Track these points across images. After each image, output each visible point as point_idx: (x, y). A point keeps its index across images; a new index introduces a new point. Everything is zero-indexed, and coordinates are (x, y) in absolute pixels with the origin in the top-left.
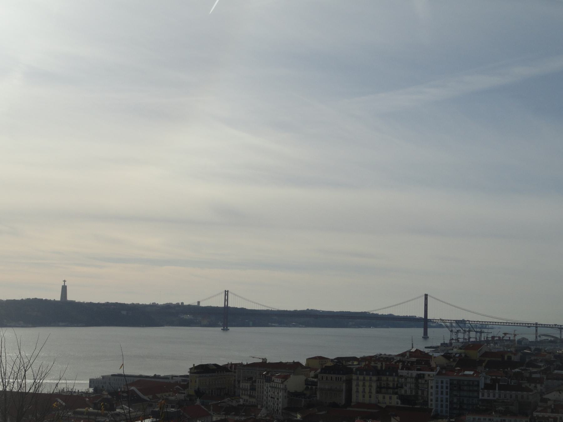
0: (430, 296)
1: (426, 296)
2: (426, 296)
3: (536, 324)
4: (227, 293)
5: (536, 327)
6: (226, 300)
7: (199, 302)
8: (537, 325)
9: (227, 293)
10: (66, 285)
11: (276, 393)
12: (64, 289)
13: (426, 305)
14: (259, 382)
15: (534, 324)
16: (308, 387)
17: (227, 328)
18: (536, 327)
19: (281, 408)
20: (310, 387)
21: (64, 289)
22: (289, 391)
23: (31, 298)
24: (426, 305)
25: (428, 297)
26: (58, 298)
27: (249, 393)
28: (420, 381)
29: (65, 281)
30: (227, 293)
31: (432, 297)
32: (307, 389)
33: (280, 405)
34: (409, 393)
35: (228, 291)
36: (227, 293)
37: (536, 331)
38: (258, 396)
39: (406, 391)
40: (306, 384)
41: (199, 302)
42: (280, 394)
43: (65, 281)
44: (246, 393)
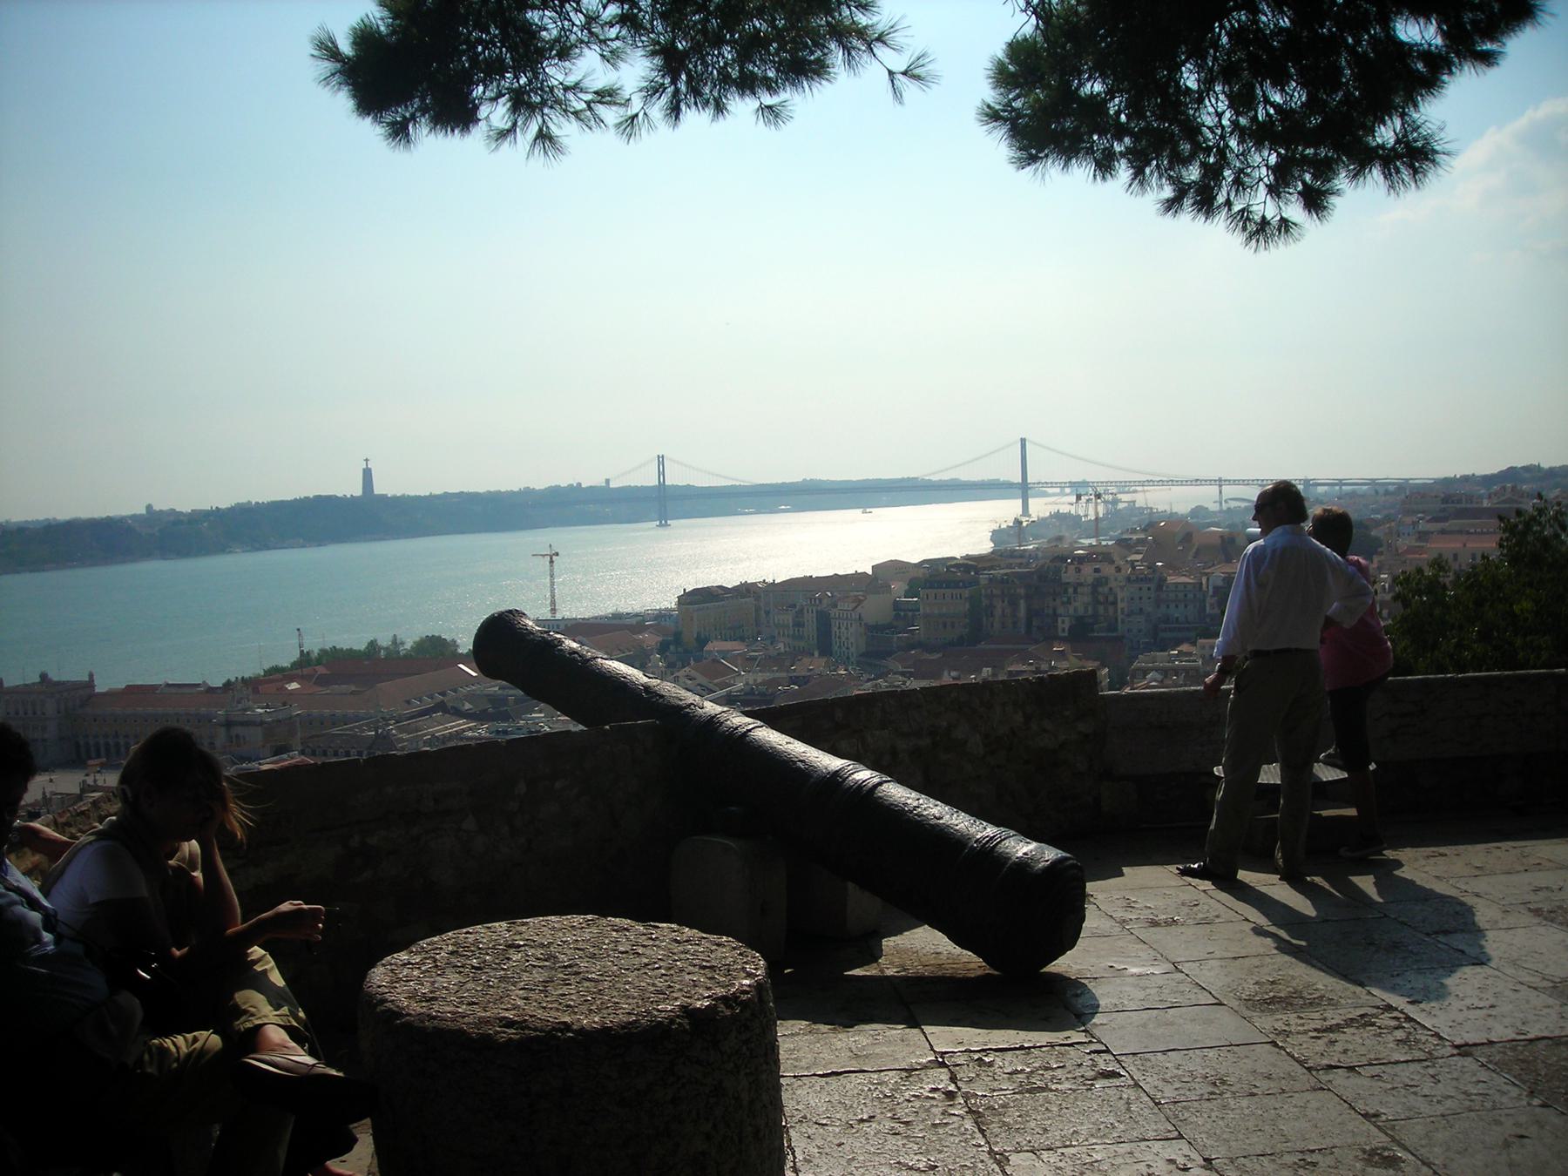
0: (1031, 442)
1: (1023, 441)
2: (1023, 441)
3: (1220, 480)
4: (661, 460)
5: (1220, 486)
6: (661, 473)
7: (607, 481)
8: (1220, 482)
9: (661, 459)
11: (843, 629)
12: (367, 474)
14: (810, 611)
15: (1215, 481)
16: (900, 615)
17: (666, 522)
18: (1220, 486)
19: (855, 655)
20: (902, 614)
21: (367, 474)
22: (865, 624)
23: (311, 496)
25: (1027, 443)
26: (358, 492)
27: (791, 632)
28: (1100, 589)
29: (367, 460)
30: (661, 459)
31: (1035, 444)
32: (897, 617)
33: (853, 649)
34: (1081, 612)
35: (663, 457)
36: (661, 460)
37: (1220, 492)
38: (809, 636)
39: (1076, 610)
40: (895, 610)
41: (607, 481)
42: (852, 630)
43: (367, 460)
44: (786, 633)
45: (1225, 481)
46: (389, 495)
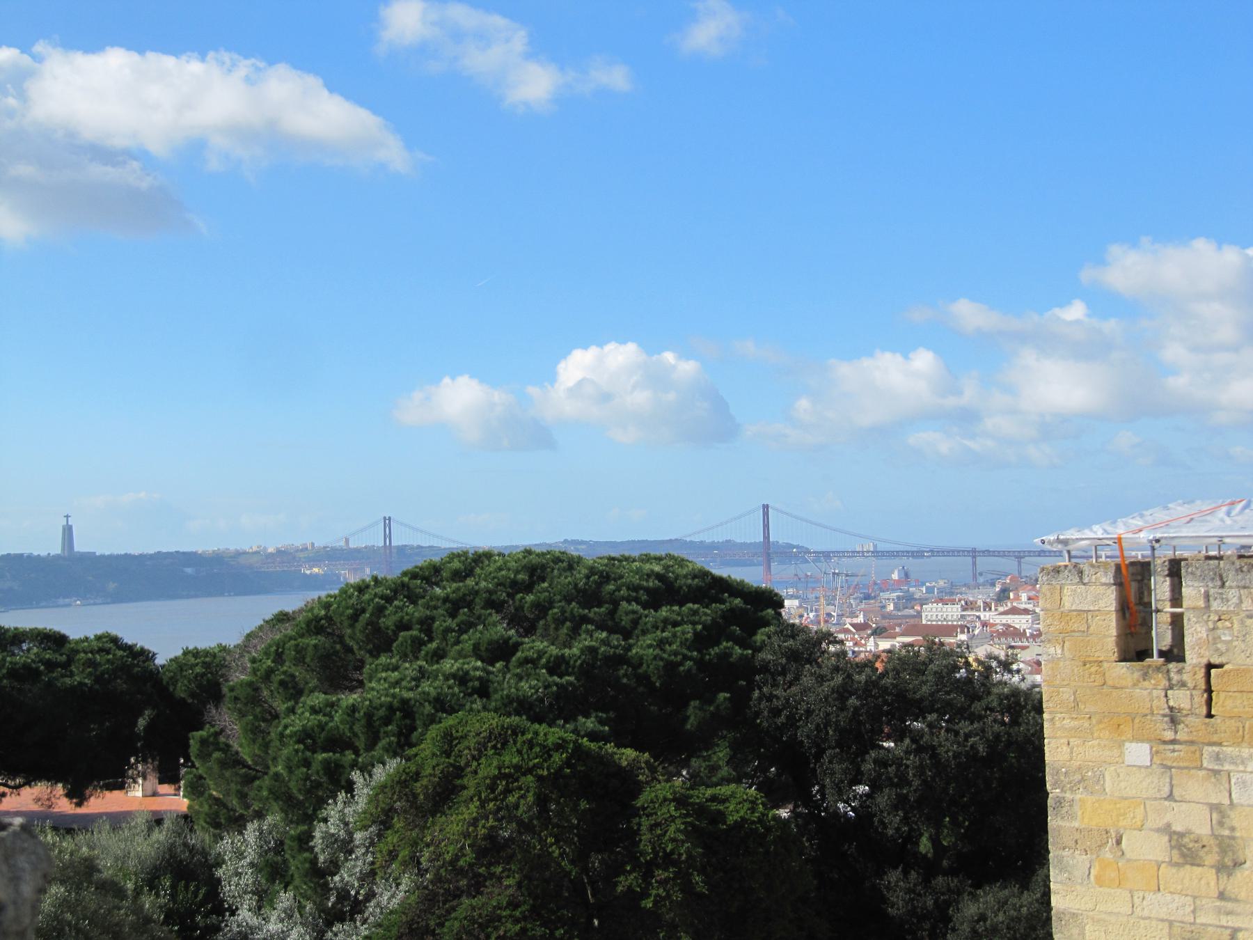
1: (766, 508)
2: (766, 508)
4: (387, 521)
5: (974, 557)
6: (388, 536)
7: (347, 541)
8: (974, 553)
9: (387, 521)
10: (70, 523)
12: (68, 531)
13: (766, 526)
15: (968, 552)
18: (974, 557)
21: (68, 531)
24: (766, 526)
26: (56, 549)
29: (67, 517)
30: (387, 521)
36: (387, 521)
37: (974, 564)
41: (347, 541)
43: (67, 517)
45: (979, 552)
46: (97, 554)
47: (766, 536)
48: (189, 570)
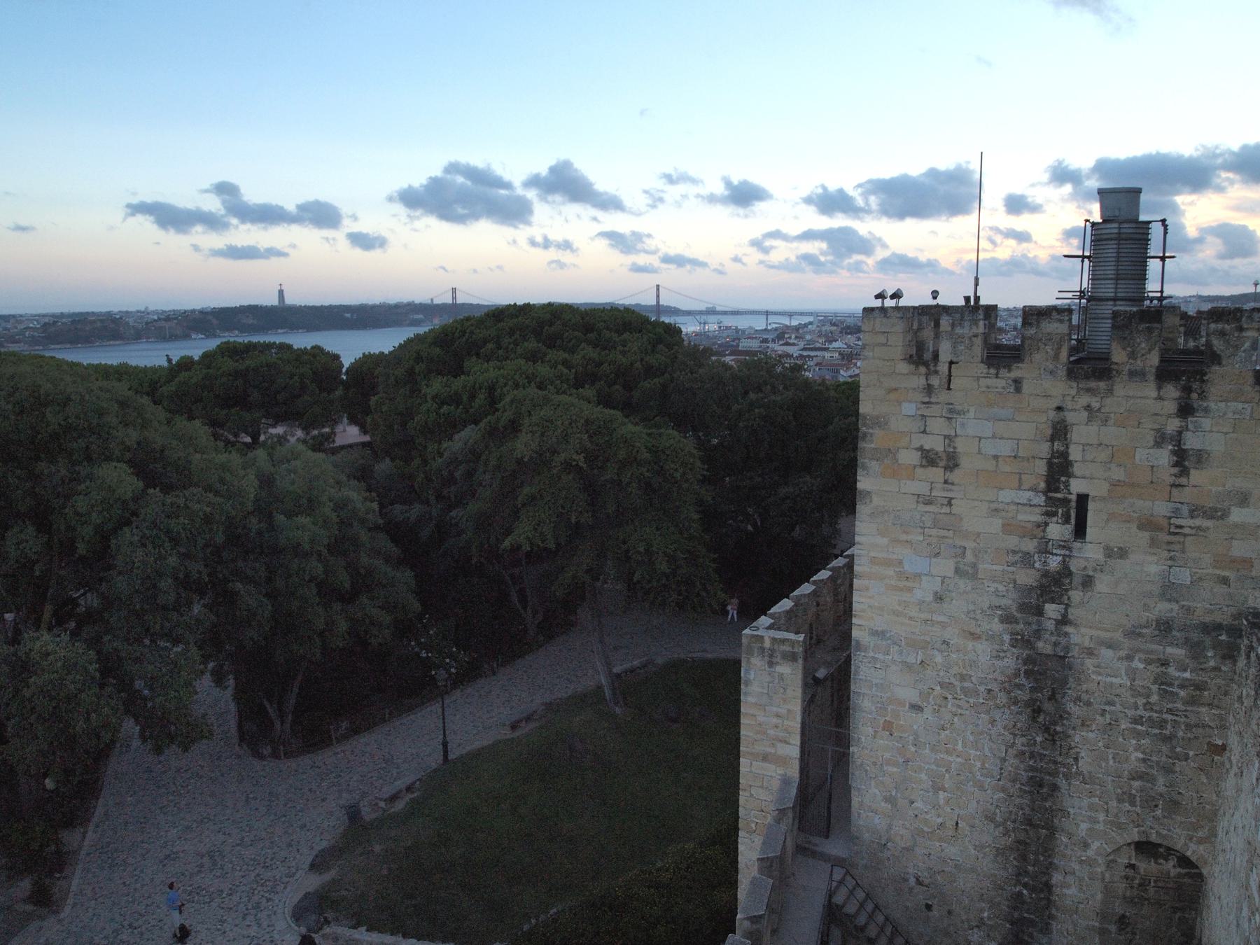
1: (658, 286)
2: (658, 286)
3: (767, 312)
4: (454, 290)
5: (767, 315)
6: (454, 298)
7: (432, 300)
8: (767, 313)
12: (281, 292)
13: (658, 296)
18: (767, 315)
21: (281, 292)
24: (658, 296)
31: (664, 288)
36: (454, 290)
37: (767, 319)
41: (432, 300)
47: (658, 301)
48: (348, 315)
